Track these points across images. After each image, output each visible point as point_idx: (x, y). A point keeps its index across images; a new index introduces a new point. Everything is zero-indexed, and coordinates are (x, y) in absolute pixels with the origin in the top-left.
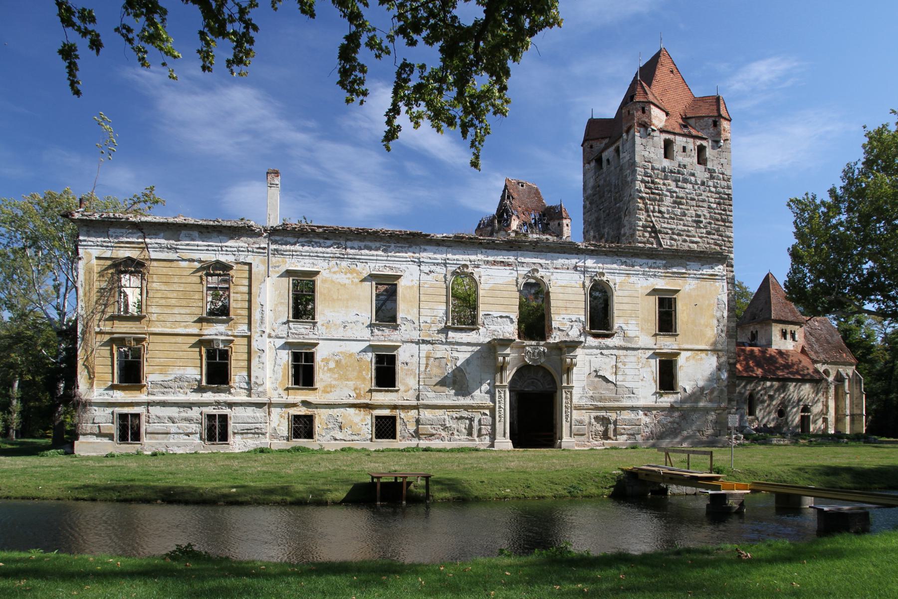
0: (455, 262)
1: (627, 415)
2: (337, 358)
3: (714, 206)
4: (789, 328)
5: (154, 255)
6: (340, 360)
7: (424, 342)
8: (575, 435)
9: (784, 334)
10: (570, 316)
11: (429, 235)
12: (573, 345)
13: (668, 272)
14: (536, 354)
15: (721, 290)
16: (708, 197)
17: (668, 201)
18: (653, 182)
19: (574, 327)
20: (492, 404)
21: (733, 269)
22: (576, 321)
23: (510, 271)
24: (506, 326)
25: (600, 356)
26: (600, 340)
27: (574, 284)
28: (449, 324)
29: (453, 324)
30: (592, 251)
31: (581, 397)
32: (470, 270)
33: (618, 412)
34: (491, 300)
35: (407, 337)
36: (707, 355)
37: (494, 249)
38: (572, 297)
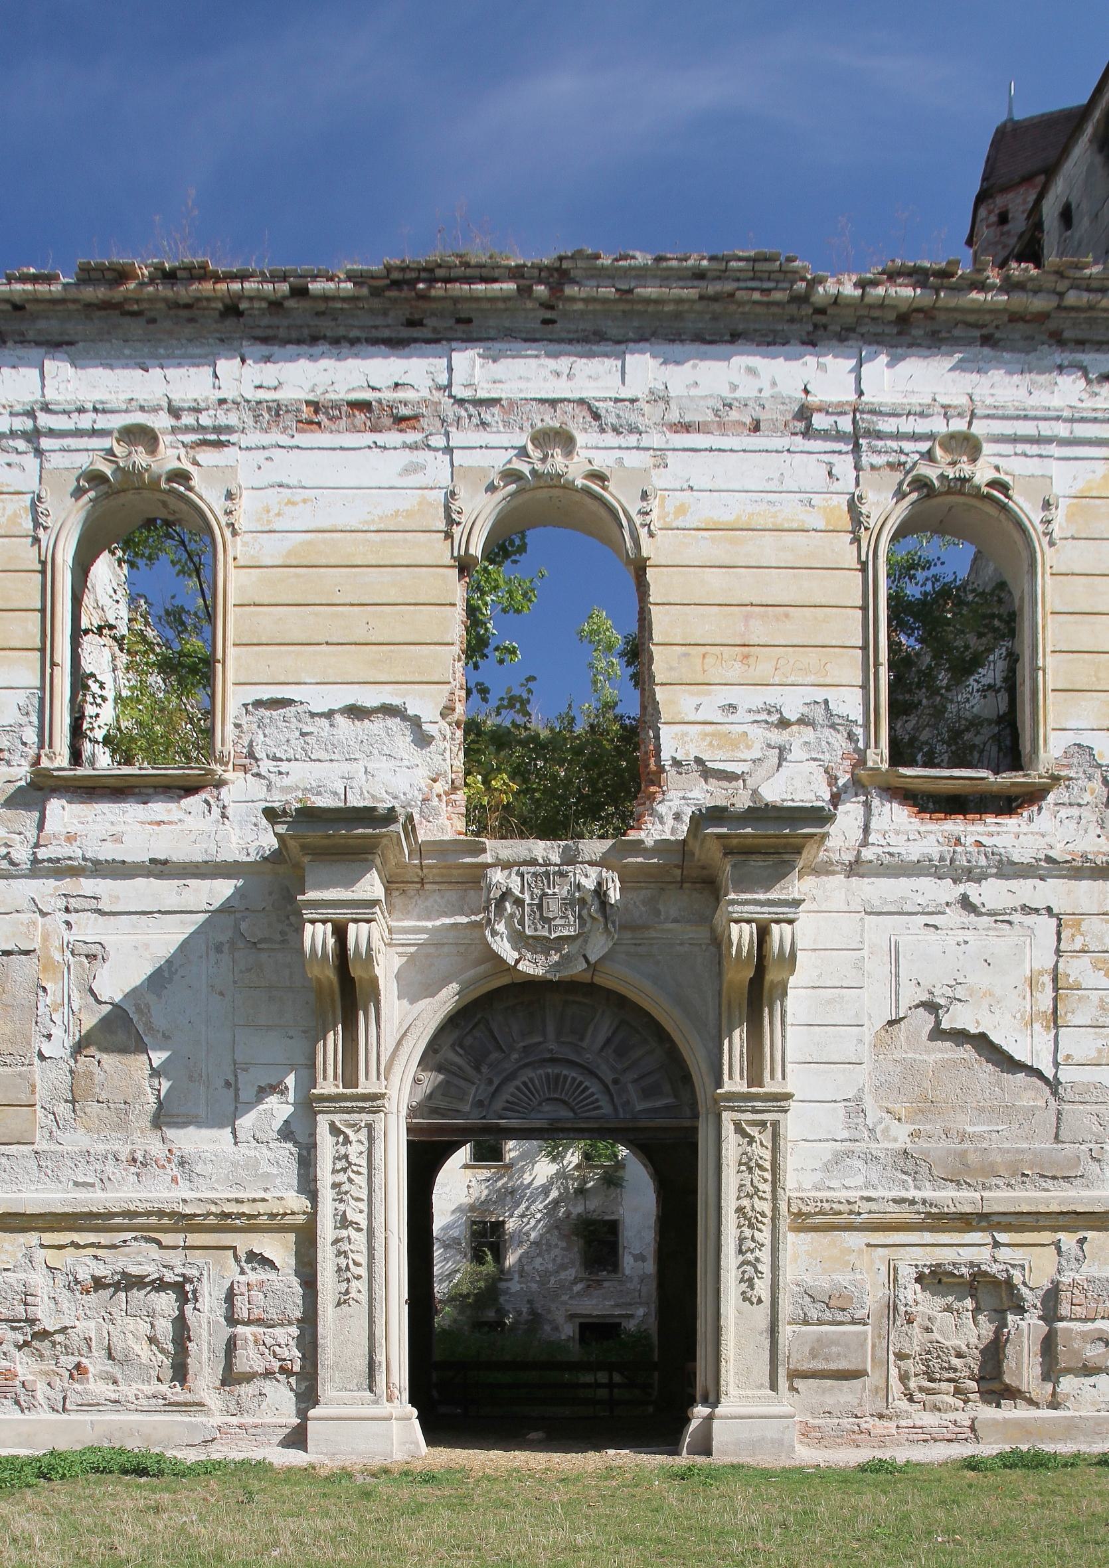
0: (85, 422)
8: (794, 1375)
10: (771, 696)
14: (553, 908)
19: (797, 753)
20: (302, 1203)
22: (803, 721)
23: (407, 456)
24: (379, 765)
25: (956, 916)
26: (955, 826)
27: (790, 510)
31: (838, 1159)
32: (169, 456)
33: (1068, 1240)
34: (295, 623)
37: (314, 340)
38: (781, 588)
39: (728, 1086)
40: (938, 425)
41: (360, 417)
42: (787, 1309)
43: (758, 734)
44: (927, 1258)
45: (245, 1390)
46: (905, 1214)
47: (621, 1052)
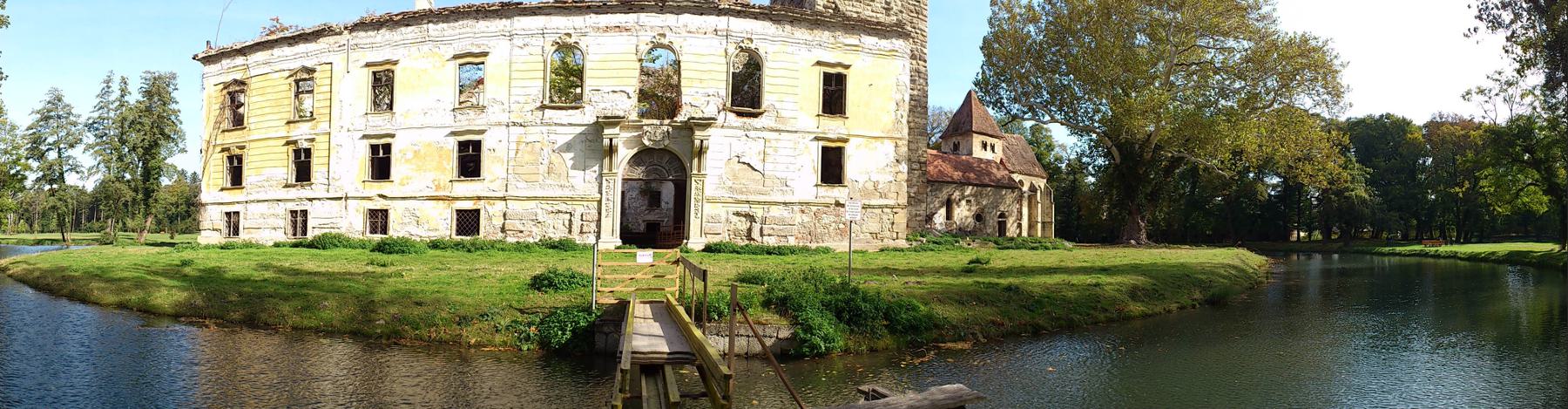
1: (776, 212)
2: (416, 148)
4: (990, 140)
6: (419, 150)
7: (514, 124)
9: (984, 146)
10: (706, 91)
12: (706, 123)
14: (657, 134)
20: (599, 196)
21: (926, 65)
28: (547, 102)
29: (552, 101)
30: (739, 12)
35: (494, 119)
36: (882, 143)
39: (694, 172)
40: (744, 35)
41: (617, 29)
42: (704, 220)
43: (704, 99)
44: (735, 210)
45: (585, 236)
46: (730, 200)
47: (670, 164)
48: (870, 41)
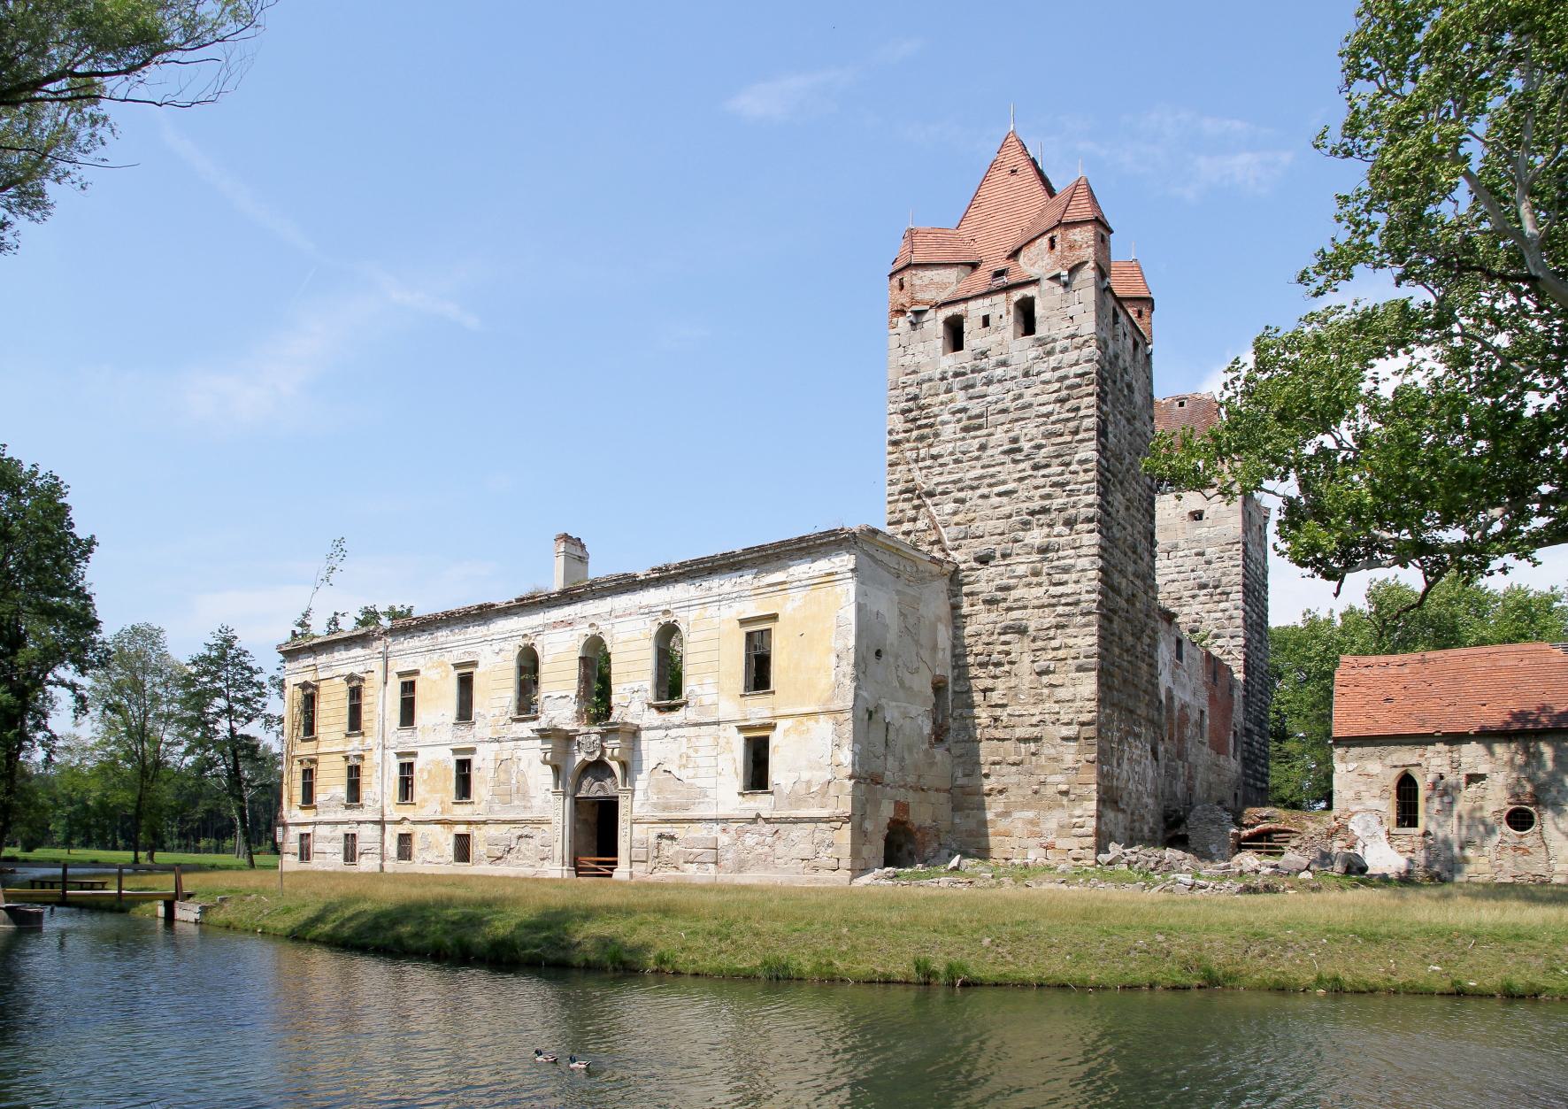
1: (699, 831)
3: (1049, 408)
5: (322, 676)
10: (632, 685)
11: (493, 605)
13: (759, 588)
15: (844, 599)
16: (1037, 395)
17: (948, 432)
18: (921, 408)
30: (658, 579)
36: (817, 722)
48: (801, 570)
